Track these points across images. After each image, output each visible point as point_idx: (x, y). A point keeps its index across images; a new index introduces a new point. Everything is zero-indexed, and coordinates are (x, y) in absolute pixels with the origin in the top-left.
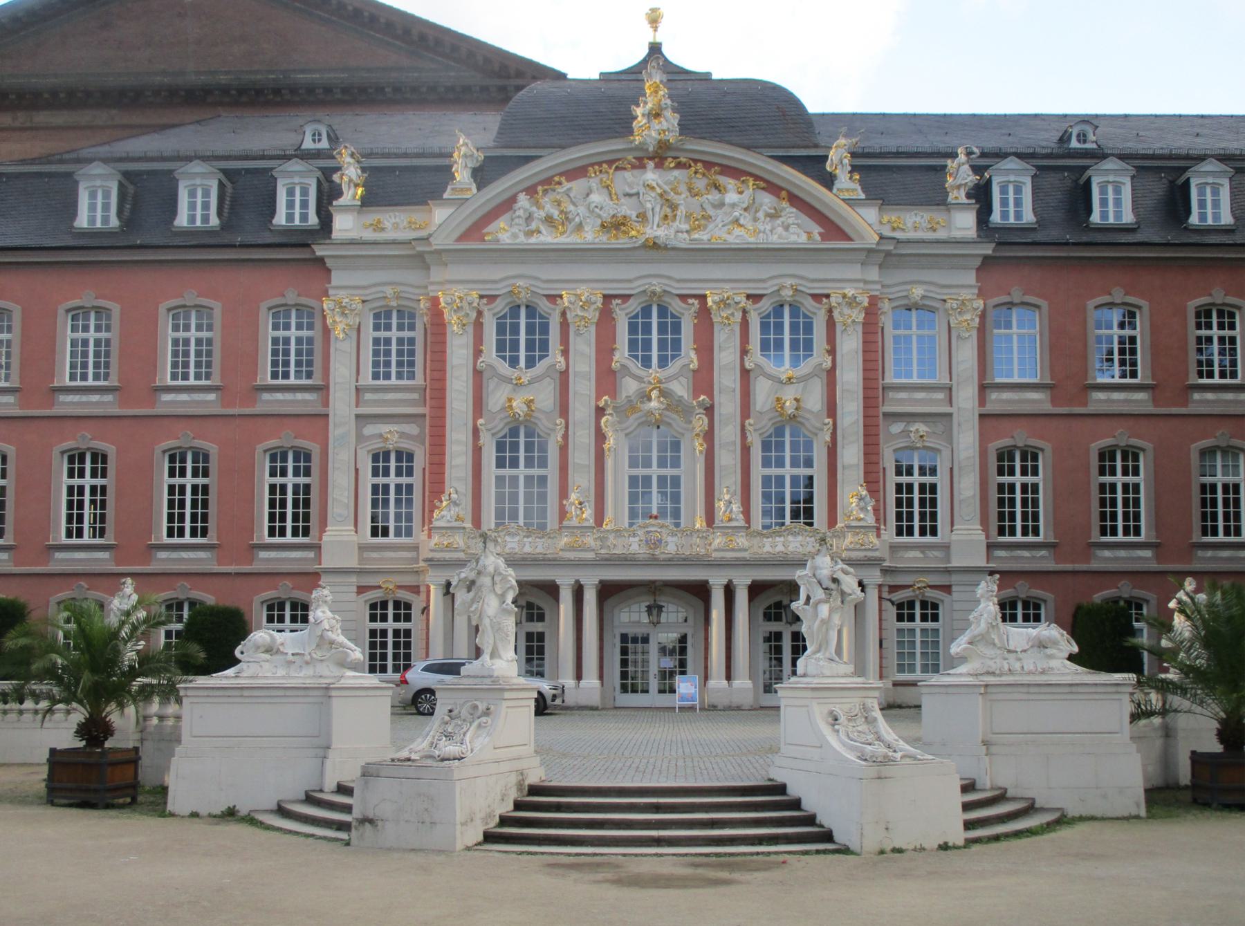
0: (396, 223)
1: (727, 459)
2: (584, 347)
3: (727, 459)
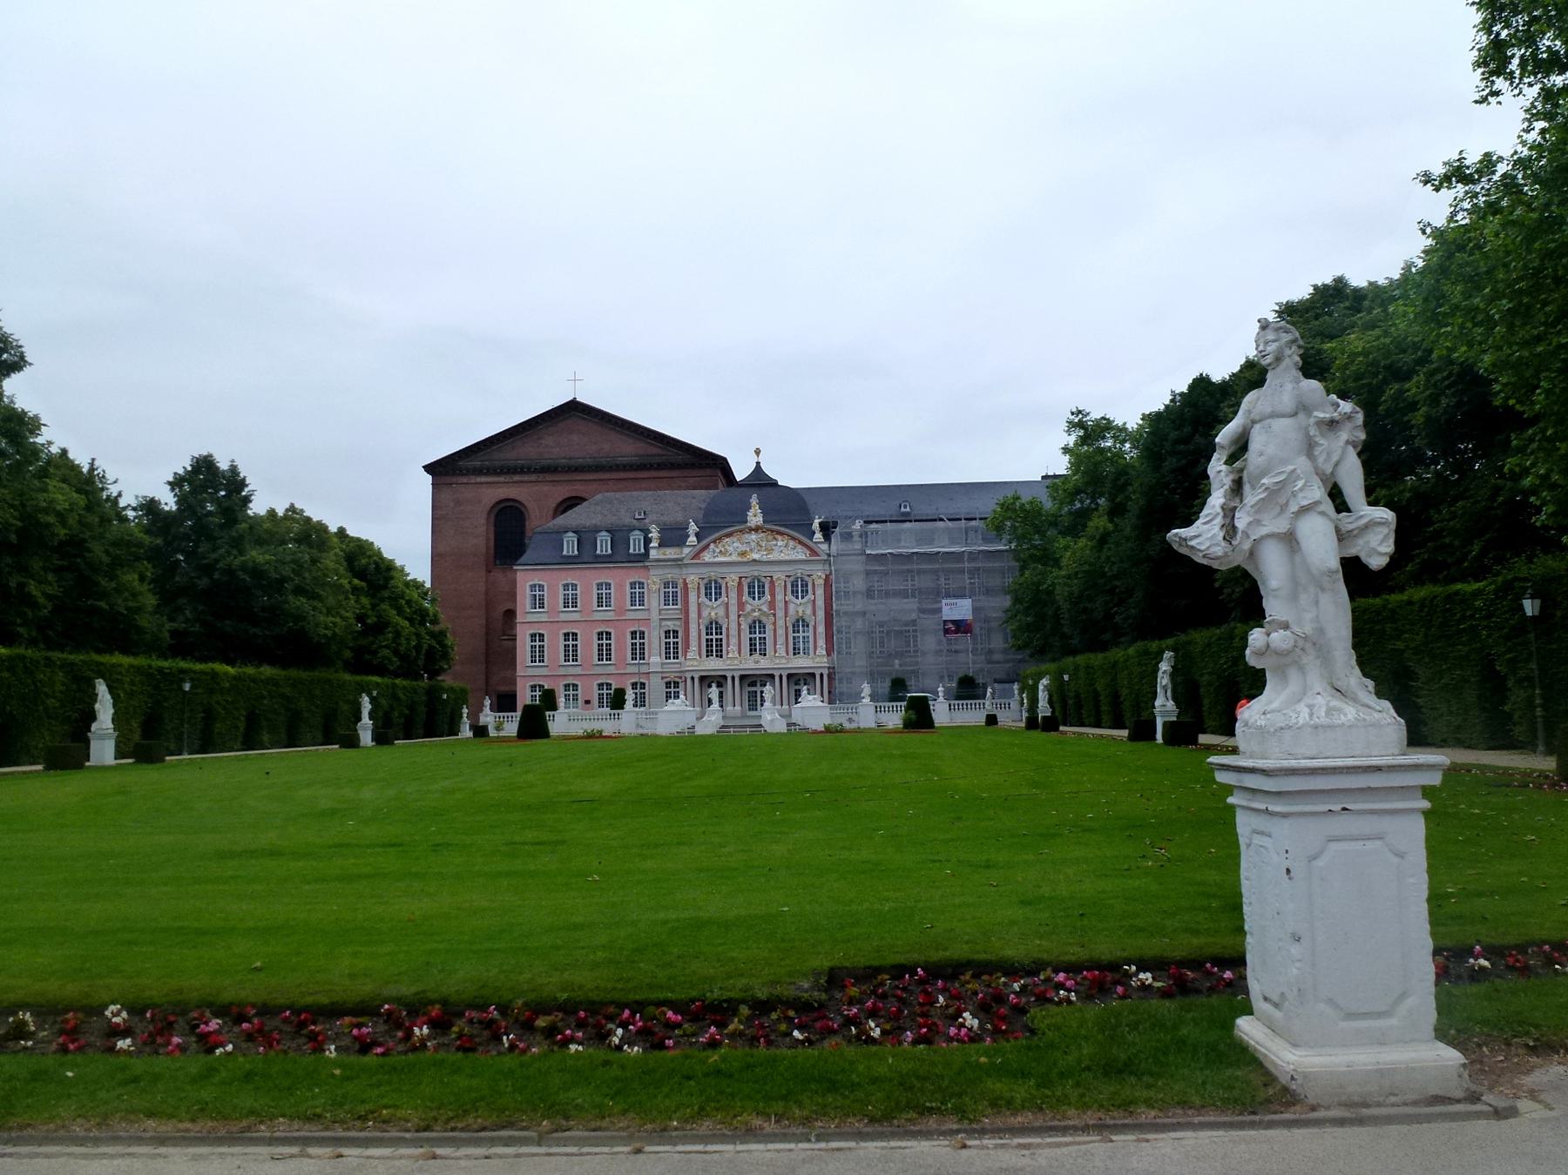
0: (671, 553)
1: (781, 632)
2: (733, 595)
3: (781, 632)
